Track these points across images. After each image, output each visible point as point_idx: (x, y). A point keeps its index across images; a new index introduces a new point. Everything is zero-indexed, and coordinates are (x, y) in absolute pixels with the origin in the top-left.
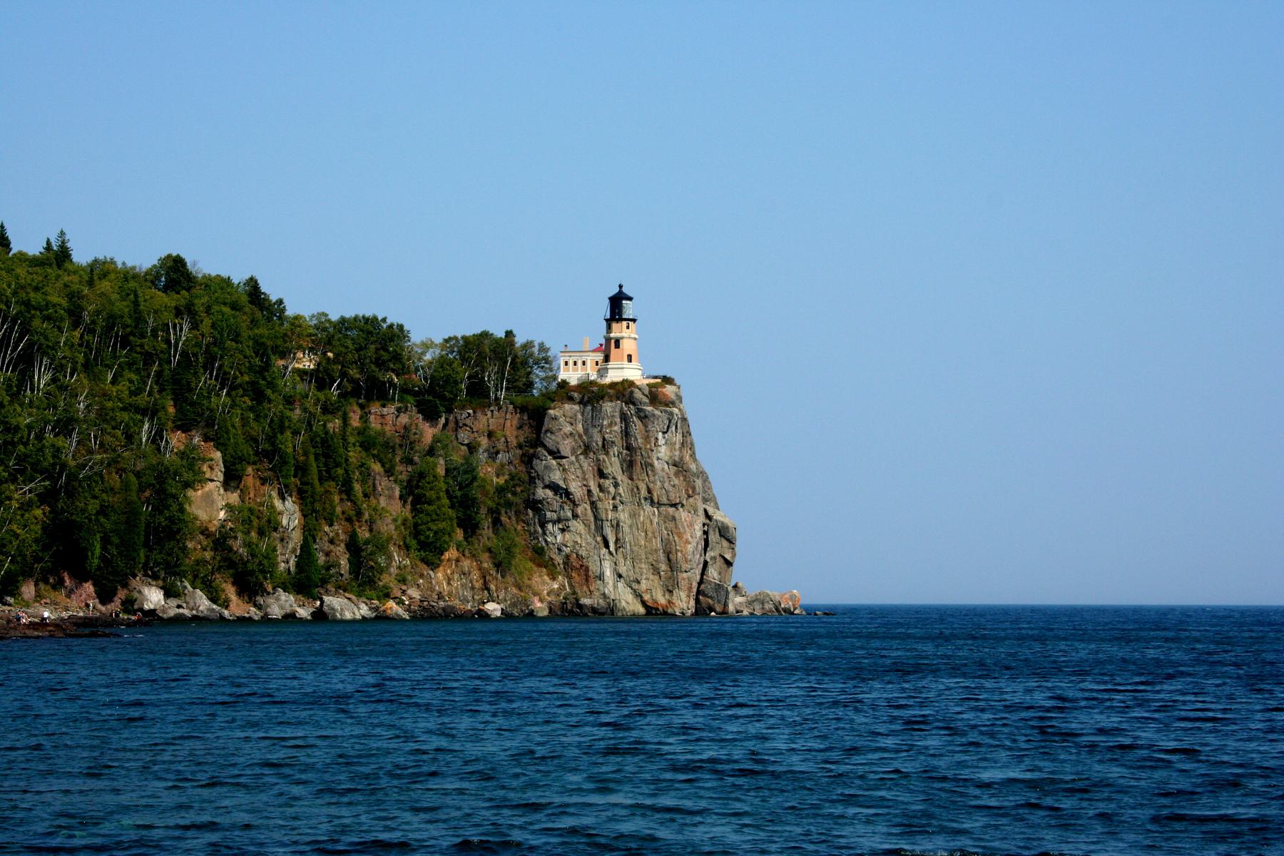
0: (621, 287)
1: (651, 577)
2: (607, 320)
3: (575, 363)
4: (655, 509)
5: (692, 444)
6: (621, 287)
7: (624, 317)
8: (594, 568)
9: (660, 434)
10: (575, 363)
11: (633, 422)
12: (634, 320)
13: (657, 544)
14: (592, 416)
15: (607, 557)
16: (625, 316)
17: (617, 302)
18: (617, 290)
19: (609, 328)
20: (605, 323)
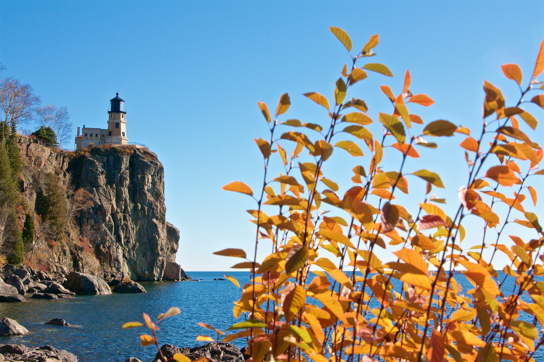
0: (117, 94)
1: (142, 259)
2: (109, 112)
3: (91, 135)
4: (146, 219)
5: (164, 182)
6: (117, 94)
7: (120, 110)
8: (114, 255)
9: (150, 176)
10: (91, 135)
11: (136, 168)
12: (125, 113)
13: (146, 240)
14: (114, 163)
15: (120, 247)
16: (120, 110)
17: (116, 103)
18: (116, 96)
19: (111, 117)
20: (108, 115)
